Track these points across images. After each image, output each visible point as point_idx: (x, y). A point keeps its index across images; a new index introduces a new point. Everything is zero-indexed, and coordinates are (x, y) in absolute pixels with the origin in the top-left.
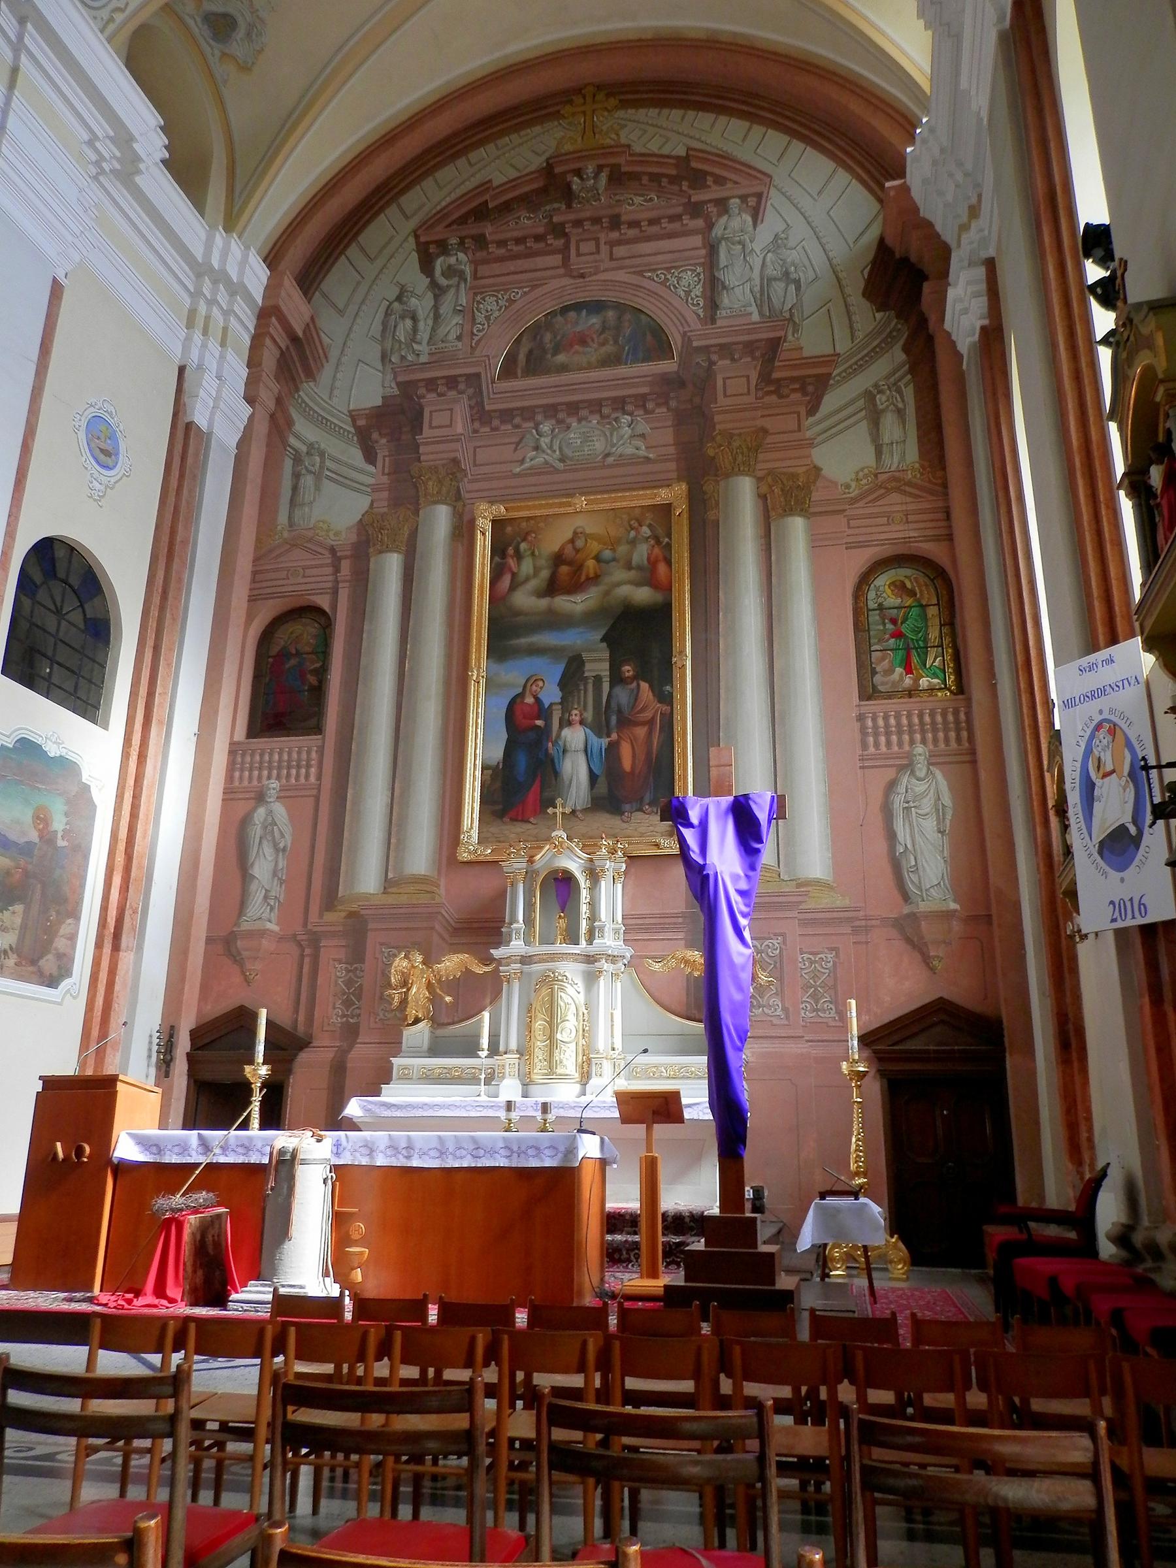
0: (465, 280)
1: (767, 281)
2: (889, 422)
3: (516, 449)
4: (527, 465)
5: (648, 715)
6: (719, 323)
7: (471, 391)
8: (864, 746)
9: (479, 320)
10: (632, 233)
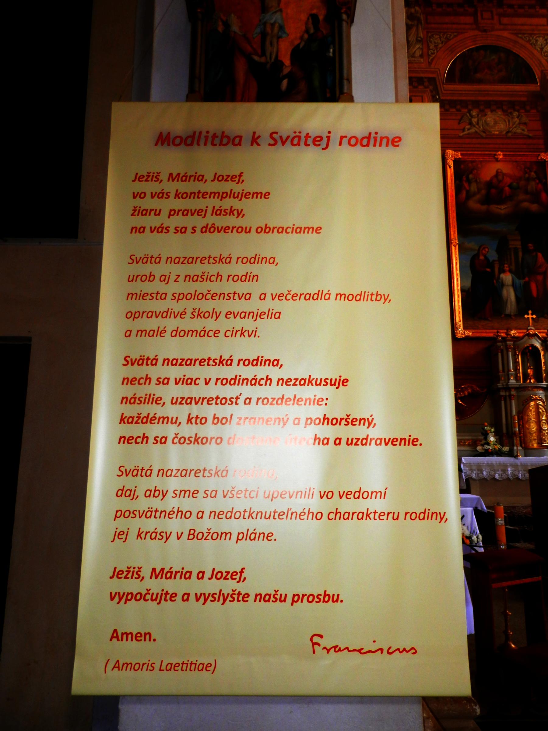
0: (421, 25)
3: (459, 123)
4: (466, 132)
7: (431, 87)
9: (431, 47)
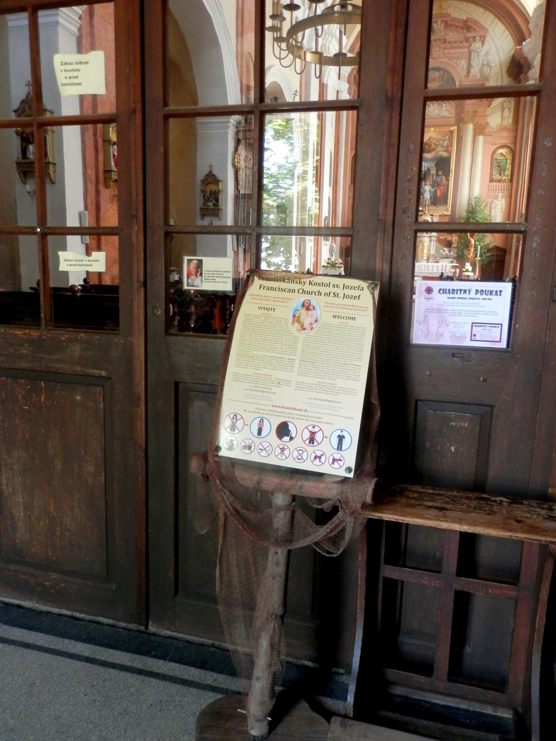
1: (483, 65)
2: (506, 111)
5: (444, 184)
6: (470, 78)
8: (488, 193)
10: (449, 46)
